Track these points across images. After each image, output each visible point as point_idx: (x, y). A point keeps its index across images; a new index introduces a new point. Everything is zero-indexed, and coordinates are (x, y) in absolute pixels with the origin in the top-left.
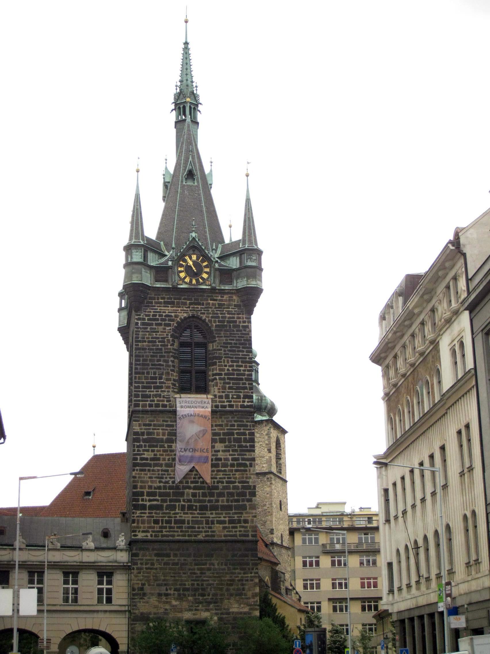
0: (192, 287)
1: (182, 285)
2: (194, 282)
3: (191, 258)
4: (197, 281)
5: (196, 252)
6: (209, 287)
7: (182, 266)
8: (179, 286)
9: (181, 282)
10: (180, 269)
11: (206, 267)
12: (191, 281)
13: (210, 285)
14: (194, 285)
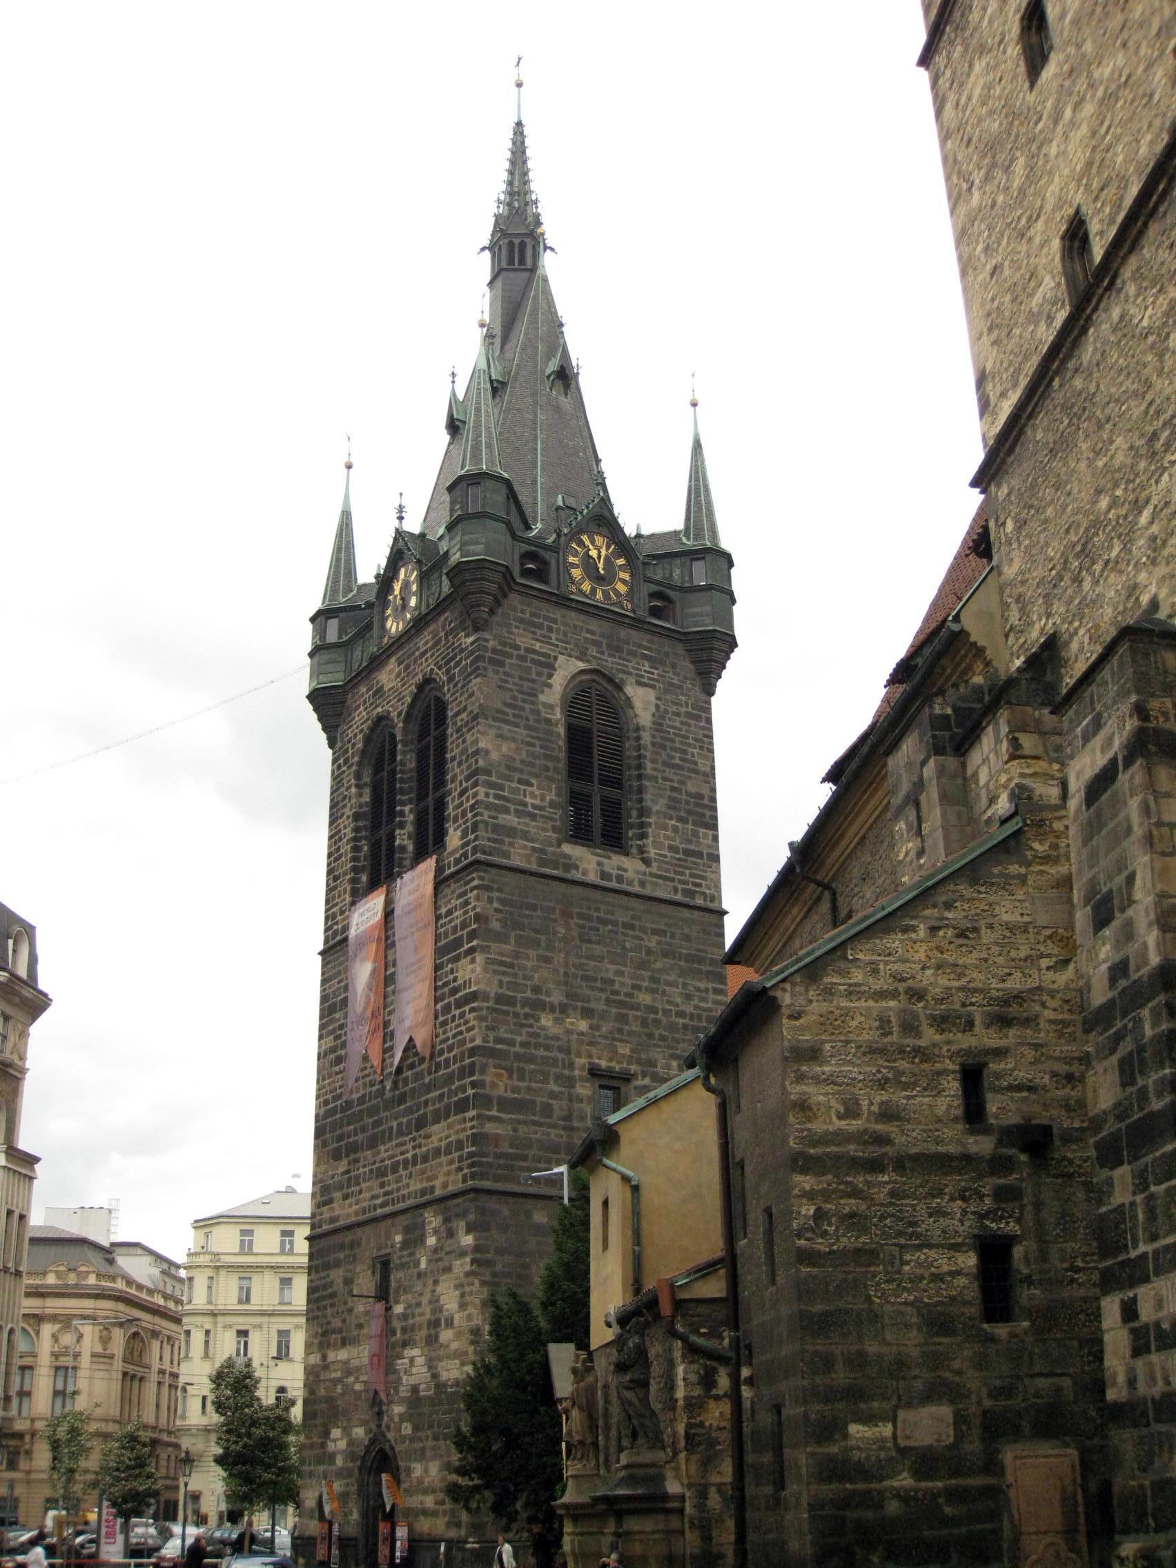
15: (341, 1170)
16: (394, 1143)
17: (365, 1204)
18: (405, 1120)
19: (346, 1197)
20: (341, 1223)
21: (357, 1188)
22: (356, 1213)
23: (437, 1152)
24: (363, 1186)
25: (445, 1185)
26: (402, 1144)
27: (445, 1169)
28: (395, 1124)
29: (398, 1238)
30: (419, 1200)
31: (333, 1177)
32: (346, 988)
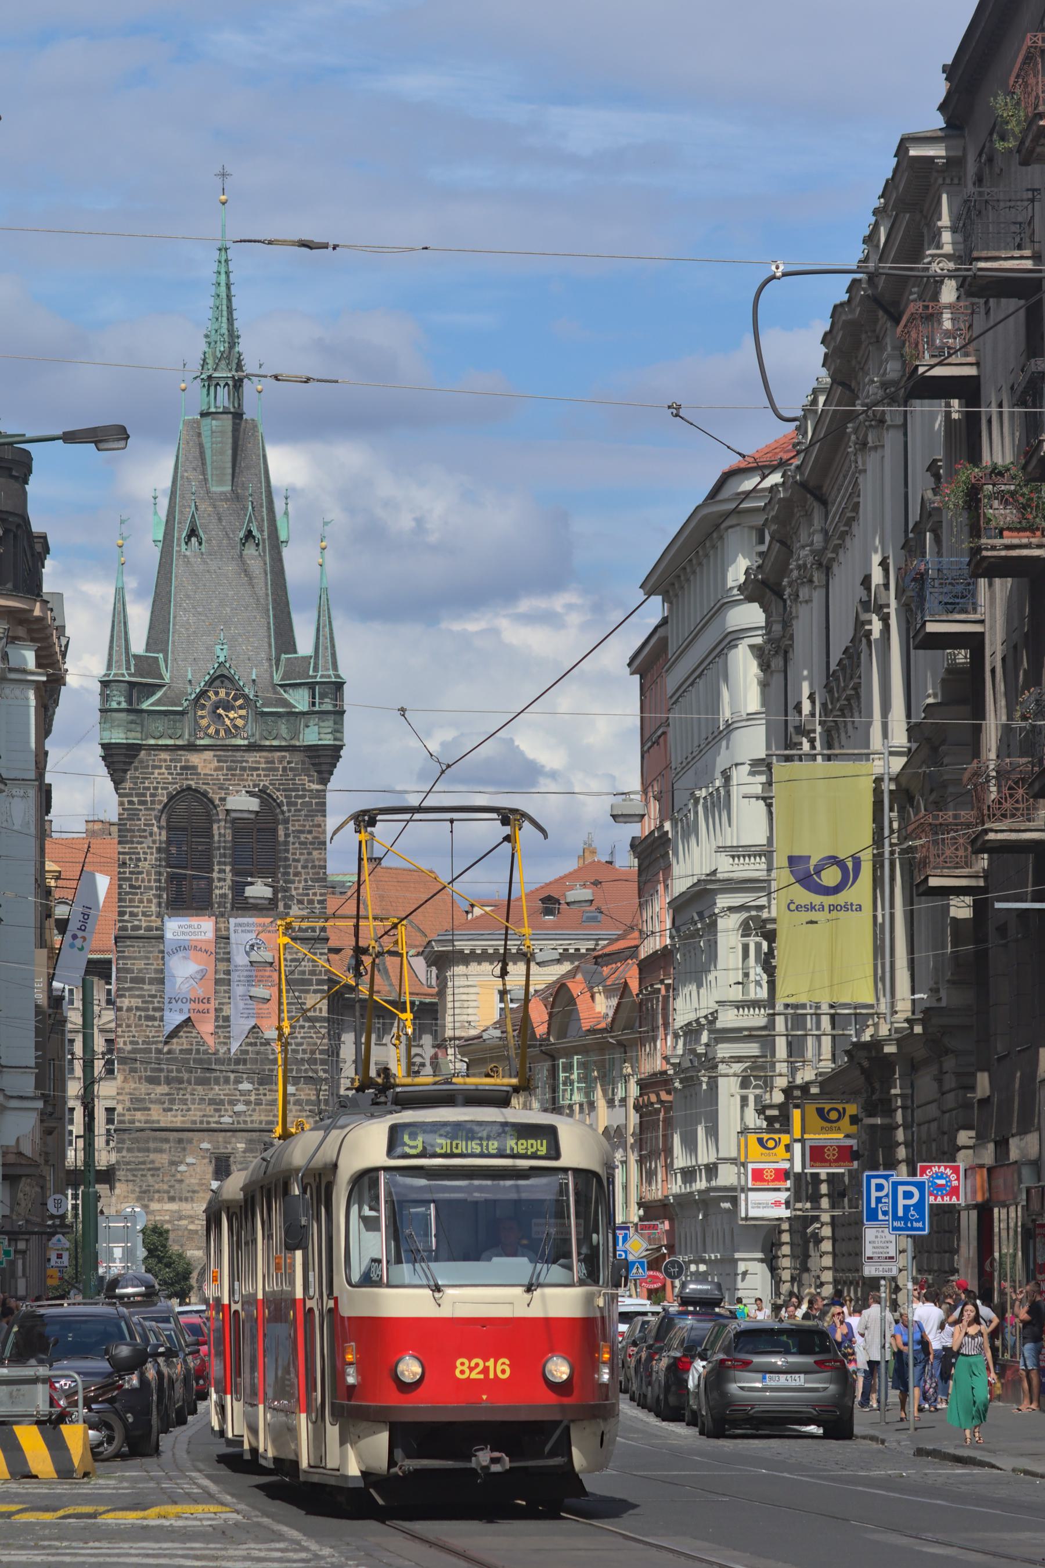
0: (219, 743)
2: (222, 733)
3: (217, 693)
5: (226, 681)
6: (246, 742)
9: (202, 734)
10: (200, 713)
11: (241, 707)
12: (217, 732)
14: (223, 739)
16: (232, 1087)
17: (198, 1119)
19: (164, 1110)
20: (162, 1125)
22: (183, 1122)
24: (193, 1107)
29: (241, 1146)
30: (263, 1126)
31: (149, 1094)
32: (162, 971)
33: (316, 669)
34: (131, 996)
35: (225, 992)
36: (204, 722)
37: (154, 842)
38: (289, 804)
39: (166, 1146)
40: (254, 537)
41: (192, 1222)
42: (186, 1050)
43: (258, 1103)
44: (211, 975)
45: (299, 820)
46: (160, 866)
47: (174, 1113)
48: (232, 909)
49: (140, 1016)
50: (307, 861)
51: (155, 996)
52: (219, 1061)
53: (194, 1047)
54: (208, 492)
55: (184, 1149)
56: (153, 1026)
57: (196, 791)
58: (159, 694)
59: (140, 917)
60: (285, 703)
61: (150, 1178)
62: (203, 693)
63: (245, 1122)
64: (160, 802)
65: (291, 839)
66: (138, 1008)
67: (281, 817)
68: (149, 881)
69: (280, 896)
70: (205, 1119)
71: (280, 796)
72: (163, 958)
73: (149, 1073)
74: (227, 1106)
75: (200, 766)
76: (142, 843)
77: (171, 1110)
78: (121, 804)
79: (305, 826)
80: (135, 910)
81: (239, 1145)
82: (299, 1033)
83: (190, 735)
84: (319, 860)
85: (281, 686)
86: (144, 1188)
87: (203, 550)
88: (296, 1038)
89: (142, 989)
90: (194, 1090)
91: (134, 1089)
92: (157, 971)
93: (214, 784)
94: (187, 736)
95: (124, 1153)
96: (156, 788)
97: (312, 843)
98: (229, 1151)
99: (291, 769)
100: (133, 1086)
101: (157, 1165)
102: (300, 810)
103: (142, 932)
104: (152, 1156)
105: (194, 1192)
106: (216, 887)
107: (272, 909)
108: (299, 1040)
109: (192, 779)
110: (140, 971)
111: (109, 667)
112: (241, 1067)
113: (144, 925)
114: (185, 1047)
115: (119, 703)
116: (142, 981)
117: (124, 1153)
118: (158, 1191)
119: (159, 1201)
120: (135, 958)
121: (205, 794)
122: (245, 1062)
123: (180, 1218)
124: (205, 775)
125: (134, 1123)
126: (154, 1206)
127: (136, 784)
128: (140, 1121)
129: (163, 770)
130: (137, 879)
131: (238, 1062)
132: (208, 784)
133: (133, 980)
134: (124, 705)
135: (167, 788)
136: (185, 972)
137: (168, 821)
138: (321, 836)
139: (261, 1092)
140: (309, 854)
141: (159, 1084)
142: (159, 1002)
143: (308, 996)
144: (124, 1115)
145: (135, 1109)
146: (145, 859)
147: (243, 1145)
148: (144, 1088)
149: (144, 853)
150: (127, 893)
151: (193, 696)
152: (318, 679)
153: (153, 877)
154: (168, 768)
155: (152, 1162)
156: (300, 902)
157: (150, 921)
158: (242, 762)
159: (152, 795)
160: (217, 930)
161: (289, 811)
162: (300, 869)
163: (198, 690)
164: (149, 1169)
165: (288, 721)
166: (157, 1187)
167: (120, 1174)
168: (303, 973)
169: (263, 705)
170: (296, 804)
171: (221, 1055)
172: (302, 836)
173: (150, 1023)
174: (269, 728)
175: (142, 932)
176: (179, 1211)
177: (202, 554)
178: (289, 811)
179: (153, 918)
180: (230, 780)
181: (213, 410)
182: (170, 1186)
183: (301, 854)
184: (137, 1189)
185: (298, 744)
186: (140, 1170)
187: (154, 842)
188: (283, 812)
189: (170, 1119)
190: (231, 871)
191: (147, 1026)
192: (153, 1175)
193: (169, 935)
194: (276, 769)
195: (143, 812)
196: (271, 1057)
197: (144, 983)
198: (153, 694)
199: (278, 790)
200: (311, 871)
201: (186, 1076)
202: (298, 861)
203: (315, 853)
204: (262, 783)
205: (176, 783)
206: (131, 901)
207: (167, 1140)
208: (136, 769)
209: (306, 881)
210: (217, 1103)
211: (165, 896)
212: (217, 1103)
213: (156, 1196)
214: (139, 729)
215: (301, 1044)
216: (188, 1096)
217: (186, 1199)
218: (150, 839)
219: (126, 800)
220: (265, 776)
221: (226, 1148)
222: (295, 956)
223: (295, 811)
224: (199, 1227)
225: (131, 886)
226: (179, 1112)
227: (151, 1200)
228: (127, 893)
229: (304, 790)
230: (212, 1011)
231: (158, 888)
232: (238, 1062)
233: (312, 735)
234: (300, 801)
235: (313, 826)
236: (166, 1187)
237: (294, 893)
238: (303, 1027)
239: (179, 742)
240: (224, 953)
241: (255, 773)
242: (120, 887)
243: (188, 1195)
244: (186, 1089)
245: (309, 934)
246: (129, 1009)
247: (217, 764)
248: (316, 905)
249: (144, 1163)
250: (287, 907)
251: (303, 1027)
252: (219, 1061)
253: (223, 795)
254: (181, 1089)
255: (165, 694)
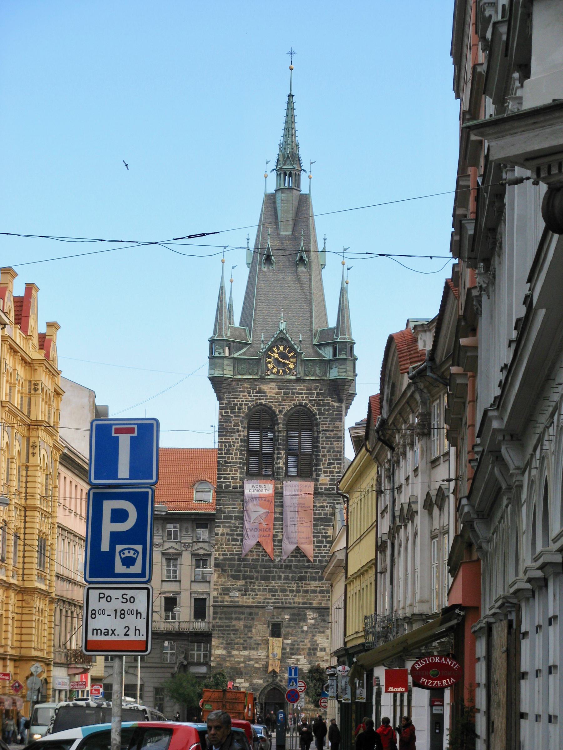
0: (279, 377)
1: (269, 375)
2: (281, 372)
4: (284, 371)
5: (284, 342)
6: (295, 378)
7: (270, 357)
8: (267, 377)
10: (268, 360)
11: (292, 357)
12: (278, 371)
13: (296, 375)
14: (281, 375)
15: (238, 584)
18: (290, 575)
19: (242, 595)
20: (240, 604)
21: (254, 593)
23: (314, 592)
24: (259, 593)
25: (318, 603)
26: (289, 584)
27: (319, 598)
28: (283, 575)
32: (242, 512)
33: (337, 335)
34: (224, 527)
35: (280, 525)
36: (270, 366)
37: (239, 436)
38: (320, 414)
39: (243, 616)
40: (304, 260)
41: (257, 663)
42: (257, 559)
43: (298, 591)
44: (272, 516)
45: (326, 424)
46: (241, 450)
47: (247, 597)
48: (285, 476)
49: (229, 539)
50: (330, 448)
51: (238, 527)
52: (275, 567)
53: (261, 558)
54: (278, 234)
55: (253, 619)
56: (236, 545)
57: (265, 405)
58: (244, 350)
59: (230, 480)
60: (319, 355)
61: (232, 635)
62: (270, 349)
63: (290, 603)
64: (244, 412)
65: (321, 435)
66: (227, 534)
67: (315, 422)
68: (236, 459)
69: (314, 469)
70: (266, 601)
71: (315, 410)
72: (243, 505)
73: (233, 573)
74: (279, 593)
75: (267, 391)
76: (232, 436)
77: (246, 595)
78: (220, 413)
79: (329, 427)
80: (227, 476)
81: (286, 617)
82: (323, 550)
83: (262, 373)
84: (338, 447)
85: (317, 345)
86: (229, 641)
87: (274, 268)
88: (322, 553)
89: (230, 523)
90: (260, 583)
91: (224, 582)
92: (239, 512)
93: (276, 402)
94: (260, 374)
95: (217, 620)
96: (241, 404)
97: (333, 438)
98: (280, 620)
99: (322, 394)
100: (223, 580)
101: (237, 628)
102: (326, 418)
103: (231, 489)
104: (234, 623)
105: (258, 644)
106: (276, 463)
107: (309, 477)
108: (323, 554)
109: (263, 399)
110: (229, 512)
111: (215, 333)
112: (288, 570)
113: (232, 485)
114: (255, 557)
115: (220, 353)
116: (230, 518)
117: (217, 620)
118: (237, 644)
119: (238, 649)
120: (226, 504)
121: (270, 408)
122: (291, 566)
123: (250, 660)
124: (271, 396)
125: (223, 602)
126: (235, 652)
127: (229, 401)
128: (227, 601)
129: (246, 394)
130: (229, 458)
131: (287, 567)
132: (272, 402)
133: (225, 518)
134: (222, 355)
135: (248, 404)
136: (256, 513)
137: (248, 424)
138: (339, 433)
139: (300, 585)
140: (332, 444)
141: (239, 579)
142: (240, 531)
143: (329, 528)
144: (217, 598)
145: (224, 594)
146: (234, 446)
147: (288, 617)
148: (229, 583)
149: (234, 442)
150: (223, 466)
151: (264, 350)
152: (338, 340)
153: (238, 456)
154: (249, 392)
155: (234, 626)
156: (325, 472)
157: (236, 483)
158: (294, 389)
159: (239, 408)
160: (276, 488)
161: (320, 418)
162: (326, 453)
163: (267, 347)
164: (233, 630)
165: (320, 365)
166: (236, 641)
167: (215, 633)
168: (326, 514)
169: (306, 356)
170: (324, 414)
171: (276, 563)
172: (328, 433)
173: (234, 543)
174: (309, 369)
175: (231, 489)
176: (249, 656)
177: (273, 270)
178: (320, 418)
179: (238, 480)
180: (285, 400)
181: (282, 187)
182: (244, 641)
183: (327, 444)
184: (225, 642)
185: (326, 379)
186: (226, 630)
187: (239, 436)
188: (316, 419)
189: (245, 600)
190: (285, 453)
191: (233, 545)
192: (234, 634)
193: (247, 492)
194: (313, 394)
195: (233, 418)
196: (307, 564)
197: (232, 520)
198: (241, 349)
199: (314, 406)
200: (332, 454)
201: (255, 575)
202: (324, 448)
203: (335, 443)
204: (304, 402)
205: (253, 401)
206: (225, 470)
207: (243, 613)
208: (230, 393)
209: (329, 460)
210: (273, 591)
211: (245, 468)
212: (273, 591)
213: (236, 646)
214: (232, 368)
215: (324, 557)
216: (256, 587)
217: (254, 649)
218: (237, 434)
219: (223, 411)
220: (306, 397)
221: (278, 618)
222: (322, 504)
223: (324, 418)
224: (261, 666)
225: (225, 462)
226: (251, 597)
227: (232, 649)
228: (223, 466)
229: (329, 406)
230: (271, 536)
231: (241, 463)
232: (287, 567)
233: (333, 374)
234: (327, 412)
235: (334, 427)
236: (241, 641)
237: (322, 467)
238: (325, 547)
239: (256, 377)
240: (280, 502)
241: (300, 396)
242: (219, 462)
243: (256, 646)
244: (254, 583)
245: (330, 491)
246: (222, 535)
247: (277, 390)
248: (335, 474)
249: (229, 626)
250: (318, 475)
251: (325, 547)
252: (275, 567)
253: (281, 409)
254: (251, 583)
255: (248, 349)
